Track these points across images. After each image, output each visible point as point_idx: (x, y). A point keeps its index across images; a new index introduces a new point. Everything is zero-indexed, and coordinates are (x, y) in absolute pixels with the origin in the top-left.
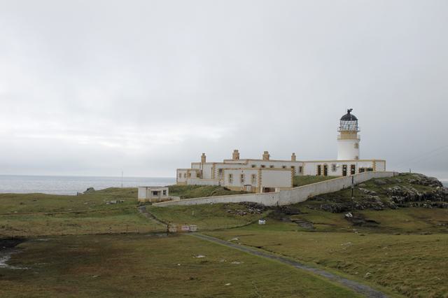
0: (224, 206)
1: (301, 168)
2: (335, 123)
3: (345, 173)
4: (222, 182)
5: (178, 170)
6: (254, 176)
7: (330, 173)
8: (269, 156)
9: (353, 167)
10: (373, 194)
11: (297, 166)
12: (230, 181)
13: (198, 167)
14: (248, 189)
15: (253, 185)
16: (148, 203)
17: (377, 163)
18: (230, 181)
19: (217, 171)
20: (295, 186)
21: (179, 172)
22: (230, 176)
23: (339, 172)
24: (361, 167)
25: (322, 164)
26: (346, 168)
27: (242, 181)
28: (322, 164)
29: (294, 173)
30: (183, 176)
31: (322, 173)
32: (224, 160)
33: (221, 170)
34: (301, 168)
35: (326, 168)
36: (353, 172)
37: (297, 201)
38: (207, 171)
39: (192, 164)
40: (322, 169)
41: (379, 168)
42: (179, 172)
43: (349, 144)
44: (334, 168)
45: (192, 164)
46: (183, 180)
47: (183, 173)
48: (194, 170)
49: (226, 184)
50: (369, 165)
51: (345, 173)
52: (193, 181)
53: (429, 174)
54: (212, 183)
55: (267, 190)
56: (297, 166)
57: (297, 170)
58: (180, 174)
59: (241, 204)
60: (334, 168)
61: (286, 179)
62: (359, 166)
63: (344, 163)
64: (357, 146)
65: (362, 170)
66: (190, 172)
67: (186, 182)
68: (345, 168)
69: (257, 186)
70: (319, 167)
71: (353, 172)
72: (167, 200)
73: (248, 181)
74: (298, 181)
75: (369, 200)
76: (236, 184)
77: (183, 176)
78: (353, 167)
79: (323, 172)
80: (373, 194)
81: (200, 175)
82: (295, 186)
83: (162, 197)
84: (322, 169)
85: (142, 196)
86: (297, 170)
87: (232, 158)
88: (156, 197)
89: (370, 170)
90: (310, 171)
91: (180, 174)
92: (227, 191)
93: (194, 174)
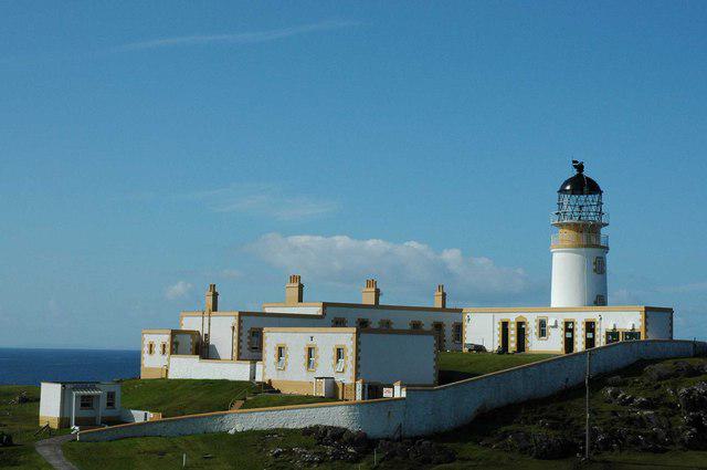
3: (569, 343)
6: (339, 353)
7: (535, 345)
9: (590, 327)
10: (643, 406)
19: (246, 335)
24: (611, 328)
25: (512, 318)
26: (572, 331)
28: (512, 318)
29: (440, 345)
31: (512, 346)
36: (590, 343)
40: (513, 333)
44: (542, 333)
49: (266, 371)
51: (569, 343)
52: (188, 368)
54: (239, 372)
59: (307, 432)
60: (542, 333)
63: (569, 316)
68: (569, 328)
70: (505, 325)
75: (630, 421)
78: (590, 327)
80: (643, 406)
84: (513, 333)
86: (449, 333)
93: (187, 341)
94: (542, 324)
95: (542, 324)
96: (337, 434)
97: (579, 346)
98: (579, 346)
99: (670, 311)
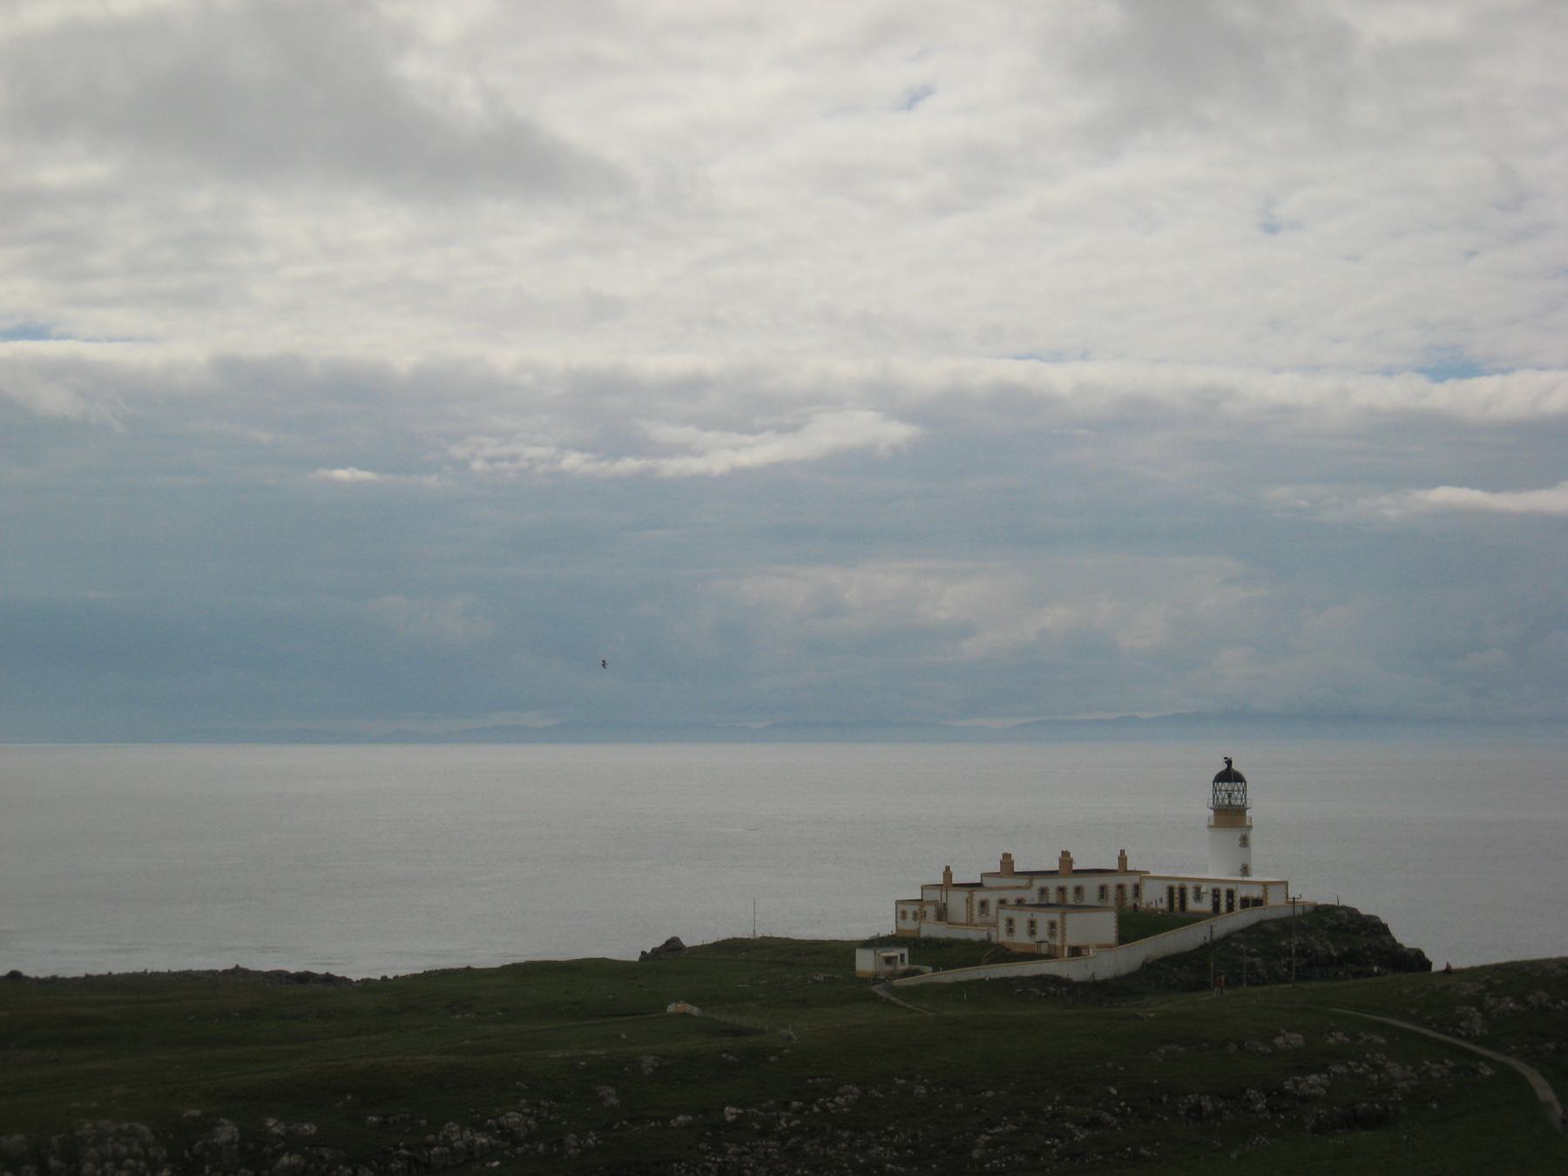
0: (1005, 984)
1: (1137, 888)
2: (1200, 804)
3: (1216, 906)
4: (994, 934)
5: (898, 902)
6: (1052, 925)
7: (1192, 905)
8: (1071, 862)
9: (1230, 894)
10: (1252, 955)
11: (1129, 881)
12: (1011, 931)
13: (935, 895)
14: (1044, 949)
15: (1052, 942)
16: (875, 979)
17: (1271, 889)
18: (1011, 931)
20: (1123, 939)
21: (901, 907)
22: (1010, 922)
23: (1206, 905)
25: (1176, 884)
27: (1032, 933)
30: (910, 916)
32: (983, 875)
33: (983, 904)
34: (1137, 888)
35: (1183, 891)
36: (1230, 908)
37: (1124, 971)
38: (957, 901)
39: (923, 888)
41: (1275, 899)
42: (901, 907)
43: (1233, 836)
44: (1198, 896)
45: (923, 888)
46: (910, 925)
47: (910, 909)
48: (930, 903)
49: (1001, 936)
50: (1256, 893)
51: (1216, 906)
52: (932, 929)
53: (1365, 907)
54: (976, 935)
55: (1076, 951)
56: (1129, 881)
57: (1129, 892)
58: (904, 914)
61: (1104, 926)
62: (1242, 892)
63: (1216, 886)
64: (1244, 842)
65: (1245, 903)
66: (926, 908)
67: (919, 931)
68: (1216, 894)
69: (1058, 943)
70: (1171, 889)
71: (1230, 908)
72: (906, 974)
73: (1042, 932)
74: (1135, 924)
76: (1021, 937)
77: (910, 916)
78: (1230, 894)
79: (1177, 894)
81: (942, 914)
82: (1123, 939)
83: (902, 967)
85: (866, 962)
86: (1129, 892)
87: (998, 870)
88: (889, 968)
89: (1258, 902)
90: (1154, 897)
91: (904, 914)
92: (1004, 954)
94: (1198, 890)
95: (1198, 890)
96: (1056, 980)
97: (1223, 908)
98: (1223, 908)
99: (1286, 883)
